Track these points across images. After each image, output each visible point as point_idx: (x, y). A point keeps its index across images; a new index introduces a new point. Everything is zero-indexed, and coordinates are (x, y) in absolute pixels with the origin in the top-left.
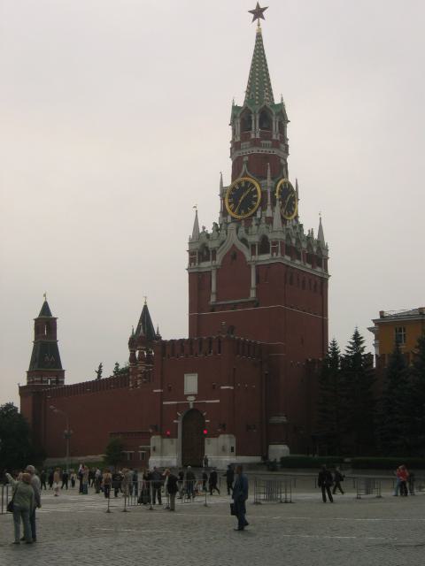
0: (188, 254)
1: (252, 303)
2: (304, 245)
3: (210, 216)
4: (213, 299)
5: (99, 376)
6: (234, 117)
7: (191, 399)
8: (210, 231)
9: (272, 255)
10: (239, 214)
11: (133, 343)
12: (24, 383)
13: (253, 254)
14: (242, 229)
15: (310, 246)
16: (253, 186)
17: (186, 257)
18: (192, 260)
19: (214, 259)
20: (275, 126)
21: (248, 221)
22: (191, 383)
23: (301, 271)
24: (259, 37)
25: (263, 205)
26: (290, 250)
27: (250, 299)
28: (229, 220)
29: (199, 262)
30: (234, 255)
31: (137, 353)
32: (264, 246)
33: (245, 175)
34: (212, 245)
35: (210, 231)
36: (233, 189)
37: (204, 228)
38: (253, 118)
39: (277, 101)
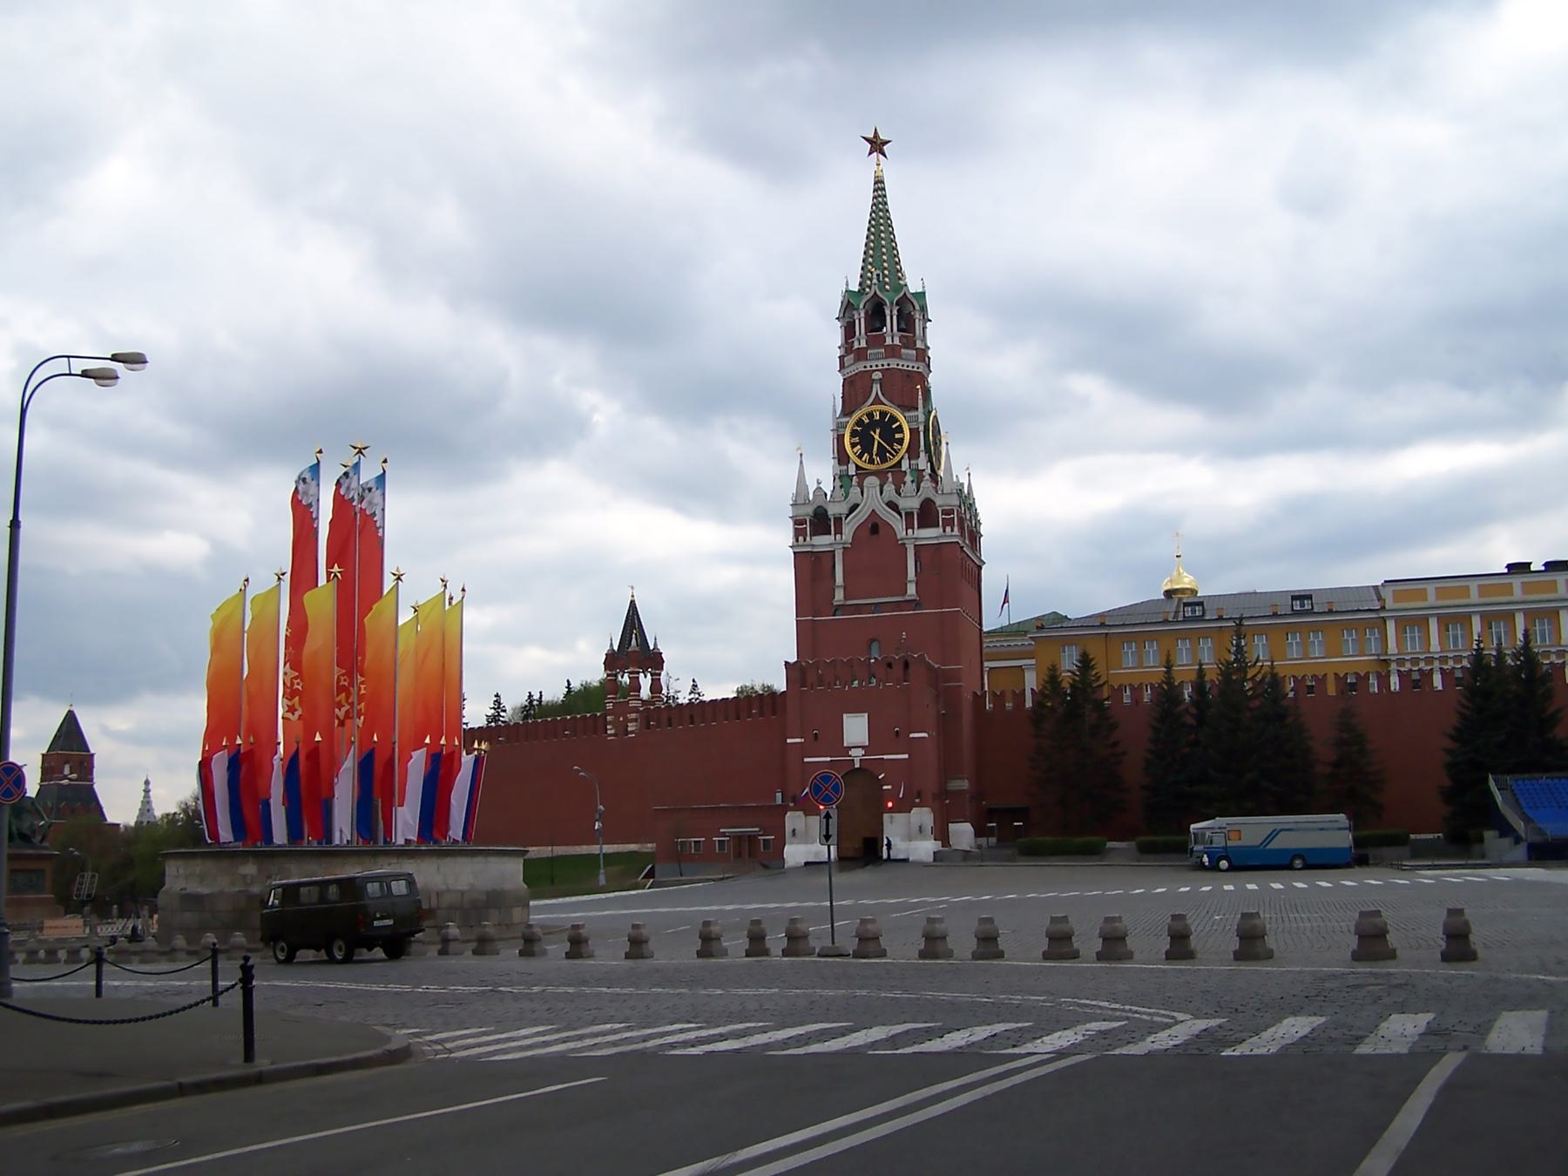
0: (791, 522)
4: (839, 595)
8: (828, 488)
13: (909, 525)
14: (889, 488)
16: (894, 419)
18: (798, 533)
19: (839, 531)
22: (856, 729)
23: (952, 550)
24: (879, 184)
25: (913, 452)
30: (874, 526)
32: (927, 514)
33: (877, 401)
34: (832, 511)
35: (828, 488)
38: (888, 312)
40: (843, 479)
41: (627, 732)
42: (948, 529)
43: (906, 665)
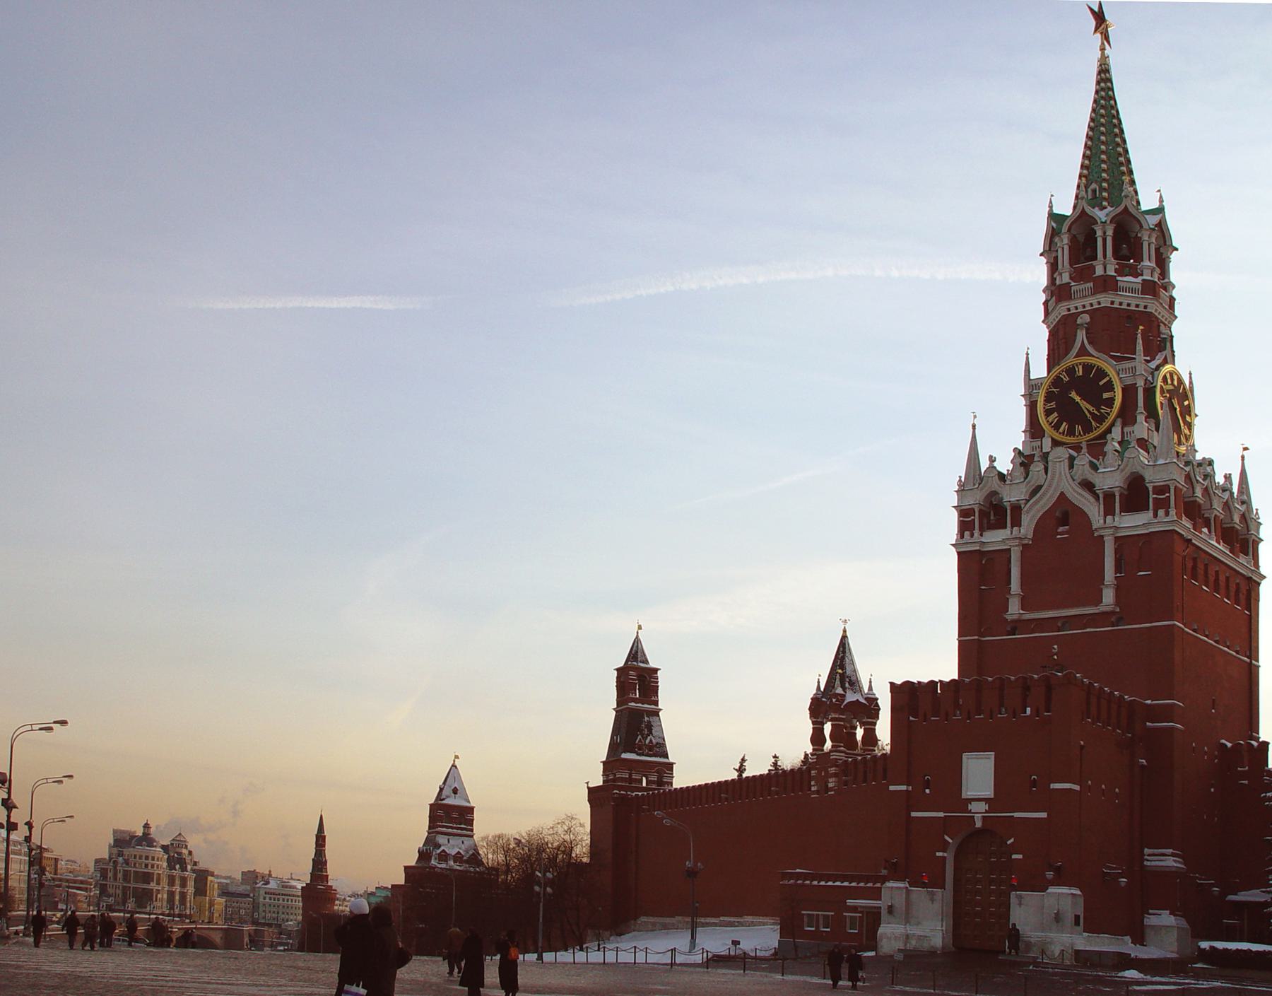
0: (955, 514)
1: (1104, 618)
2: (1217, 506)
3: (1004, 441)
4: (1014, 609)
5: (740, 775)
6: (1052, 235)
7: (979, 809)
8: (1005, 465)
9: (1156, 515)
10: (1071, 432)
11: (820, 707)
12: (598, 781)
13: (1109, 511)
14: (1083, 460)
15: (1227, 506)
16: (1102, 373)
17: (953, 519)
18: (964, 527)
19: (1017, 522)
20: (1148, 250)
21: (1097, 448)
25: (1127, 415)
26: (1192, 510)
27: (1102, 609)
28: (1047, 443)
29: (982, 530)
31: (828, 728)
32: (1136, 495)
33: (1083, 352)
34: (1011, 496)
35: (1005, 465)
36: (1056, 382)
37: (992, 460)
39: (1147, 202)
40: (1024, 460)
41: (827, 789)
42: (1161, 512)
43: (1049, 688)
